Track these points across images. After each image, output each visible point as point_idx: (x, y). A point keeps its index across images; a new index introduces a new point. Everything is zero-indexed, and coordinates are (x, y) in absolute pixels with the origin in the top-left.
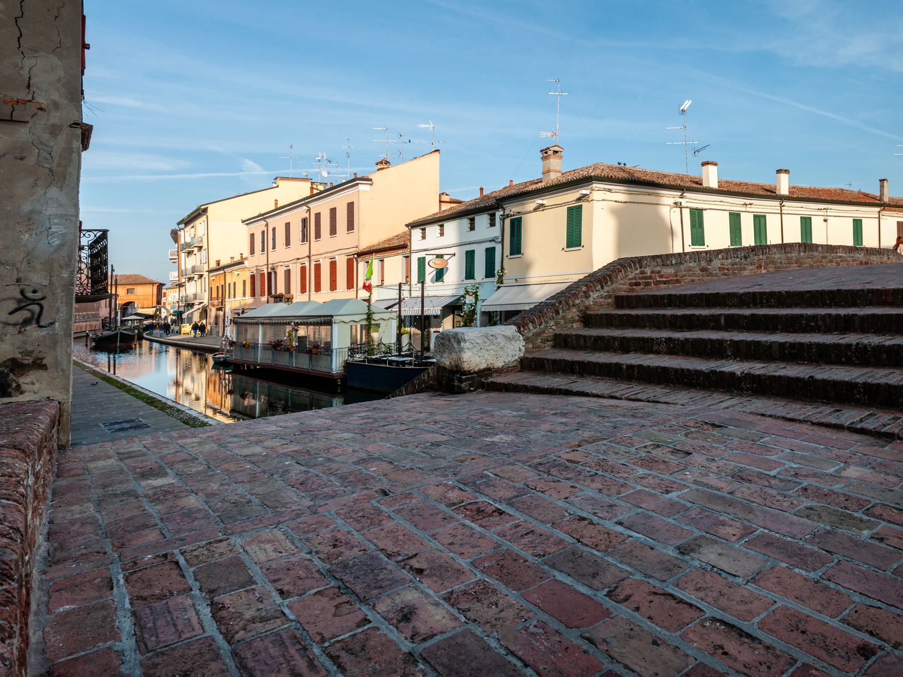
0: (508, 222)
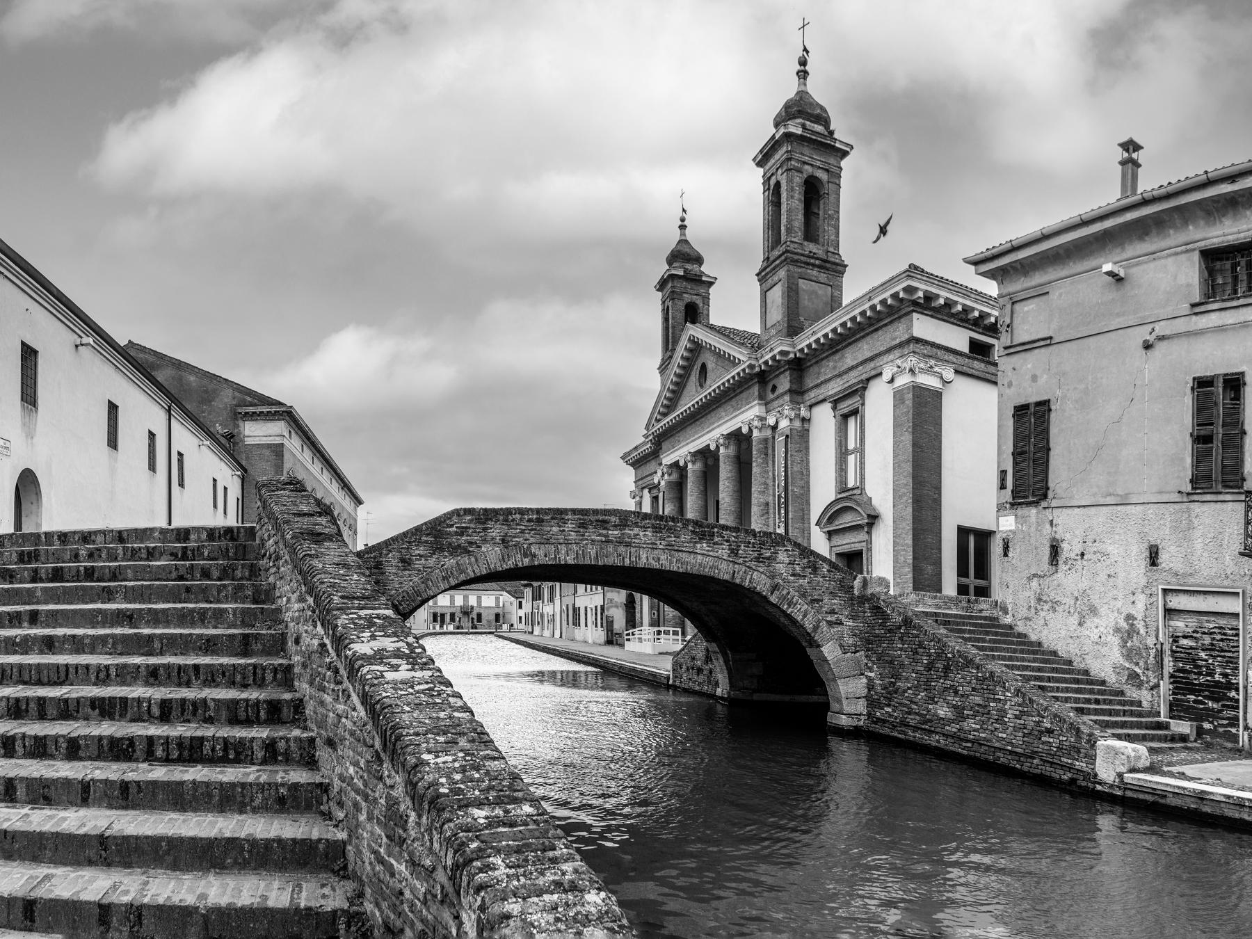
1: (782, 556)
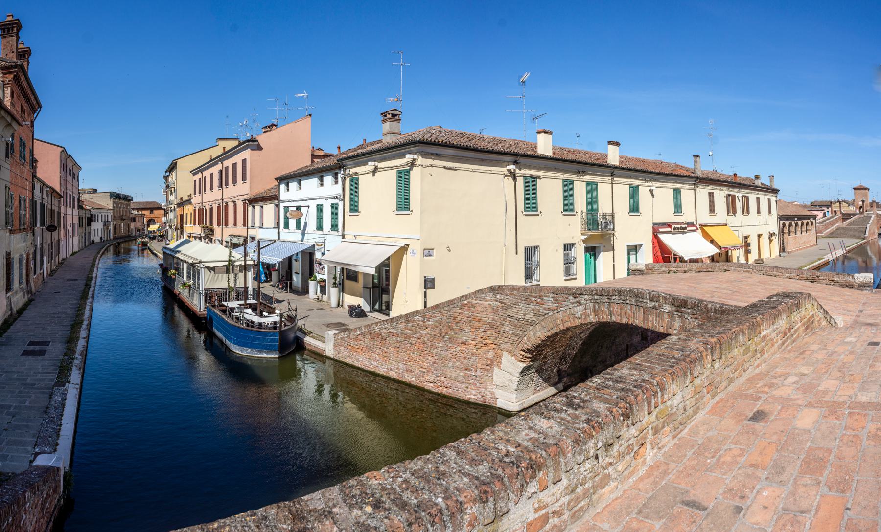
0: (348, 181)
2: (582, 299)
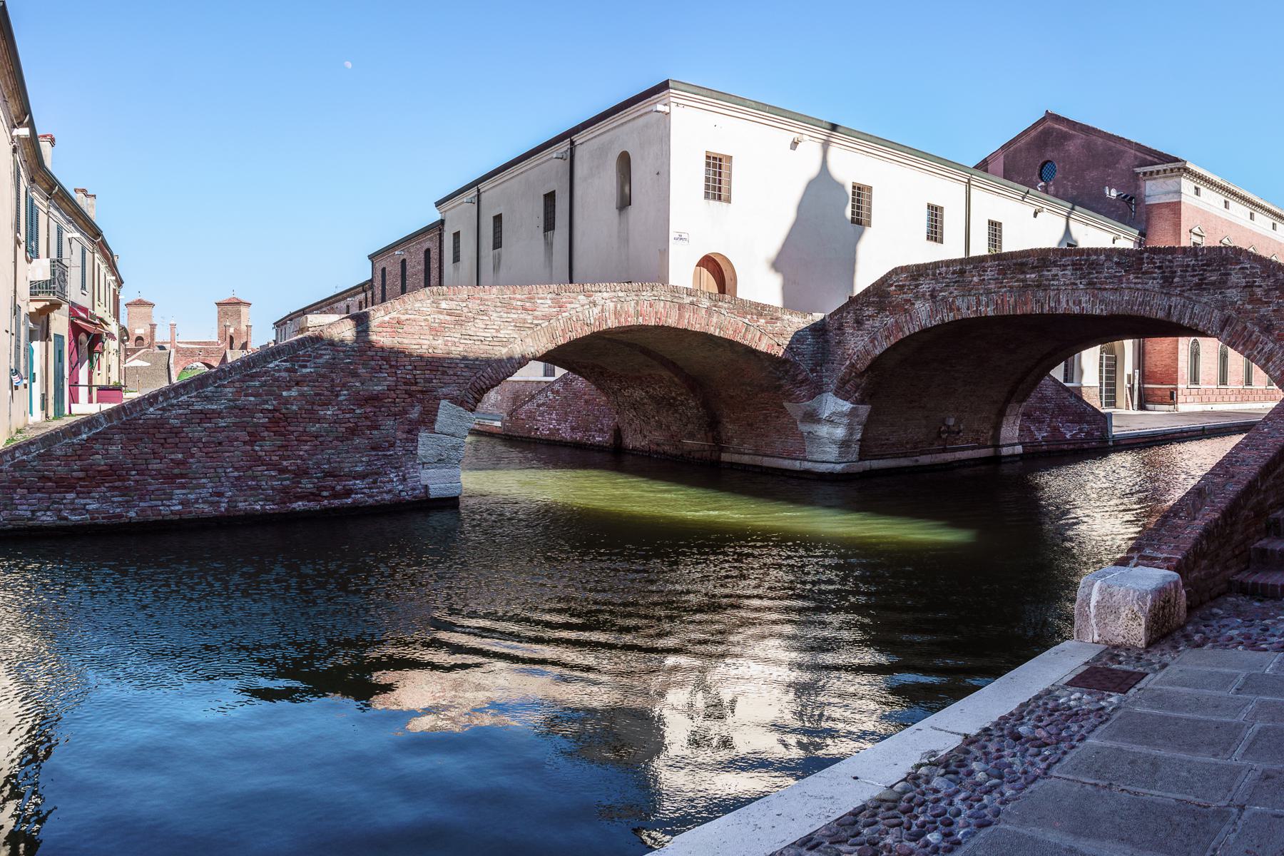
1: (1235, 278)
2: (597, 297)
